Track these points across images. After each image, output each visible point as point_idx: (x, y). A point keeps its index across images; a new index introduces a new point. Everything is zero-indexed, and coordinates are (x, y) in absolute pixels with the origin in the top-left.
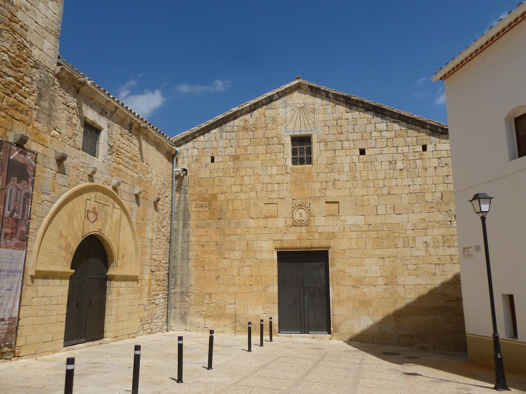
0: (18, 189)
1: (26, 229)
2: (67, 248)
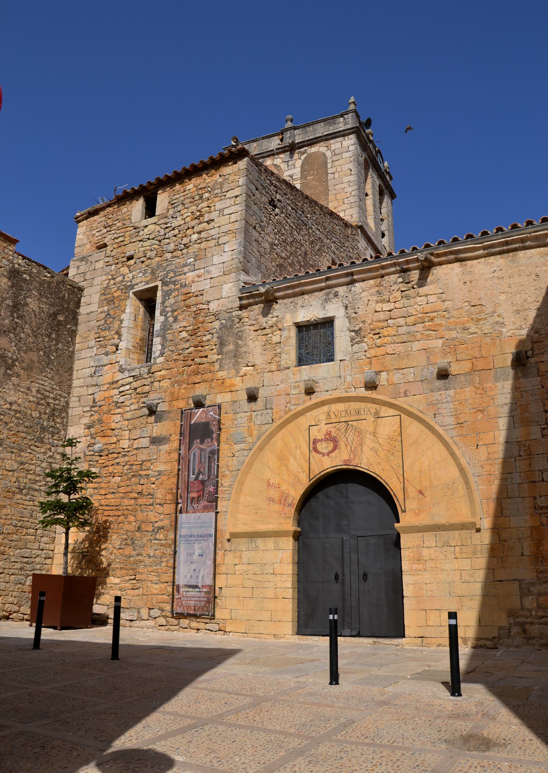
0: (202, 450)
1: (214, 489)
2: (283, 500)
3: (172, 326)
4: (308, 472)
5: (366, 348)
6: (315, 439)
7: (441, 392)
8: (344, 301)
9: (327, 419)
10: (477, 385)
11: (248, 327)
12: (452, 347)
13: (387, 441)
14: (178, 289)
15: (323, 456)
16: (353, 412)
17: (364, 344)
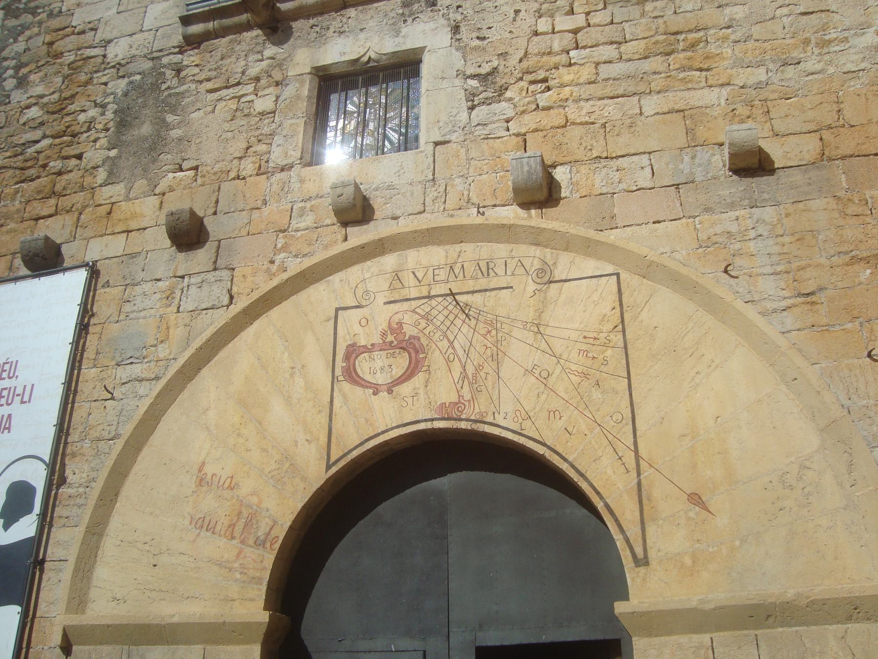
2: (242, 524)
3: (8, 96)
4: (323, 440)
5: (510, 113)
6: (353, 345)
7: (737, 213)
8: (451, 15)
9: (392, 289)
10: (842, 193)
11: (193, 86)
12: (755, 102)
13: (579, 346)
14: (40, 23)
15: (375, 394)
16: (470, 268)
17: (504, 104)
